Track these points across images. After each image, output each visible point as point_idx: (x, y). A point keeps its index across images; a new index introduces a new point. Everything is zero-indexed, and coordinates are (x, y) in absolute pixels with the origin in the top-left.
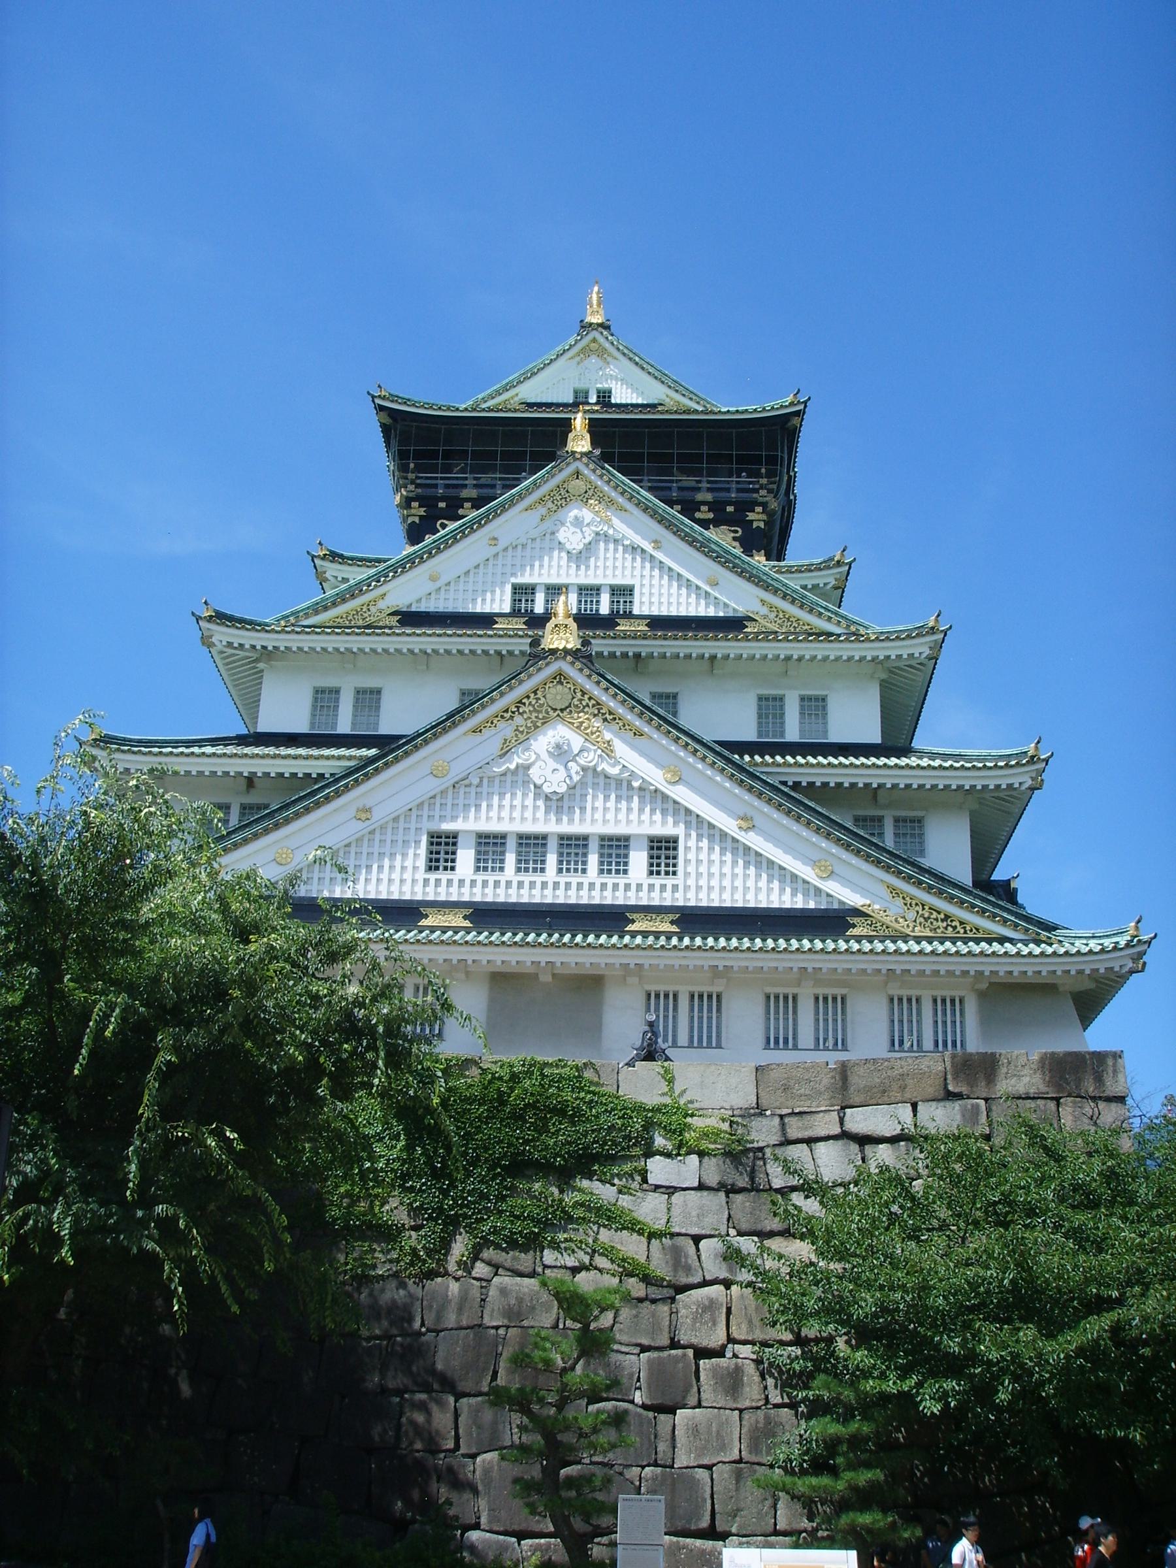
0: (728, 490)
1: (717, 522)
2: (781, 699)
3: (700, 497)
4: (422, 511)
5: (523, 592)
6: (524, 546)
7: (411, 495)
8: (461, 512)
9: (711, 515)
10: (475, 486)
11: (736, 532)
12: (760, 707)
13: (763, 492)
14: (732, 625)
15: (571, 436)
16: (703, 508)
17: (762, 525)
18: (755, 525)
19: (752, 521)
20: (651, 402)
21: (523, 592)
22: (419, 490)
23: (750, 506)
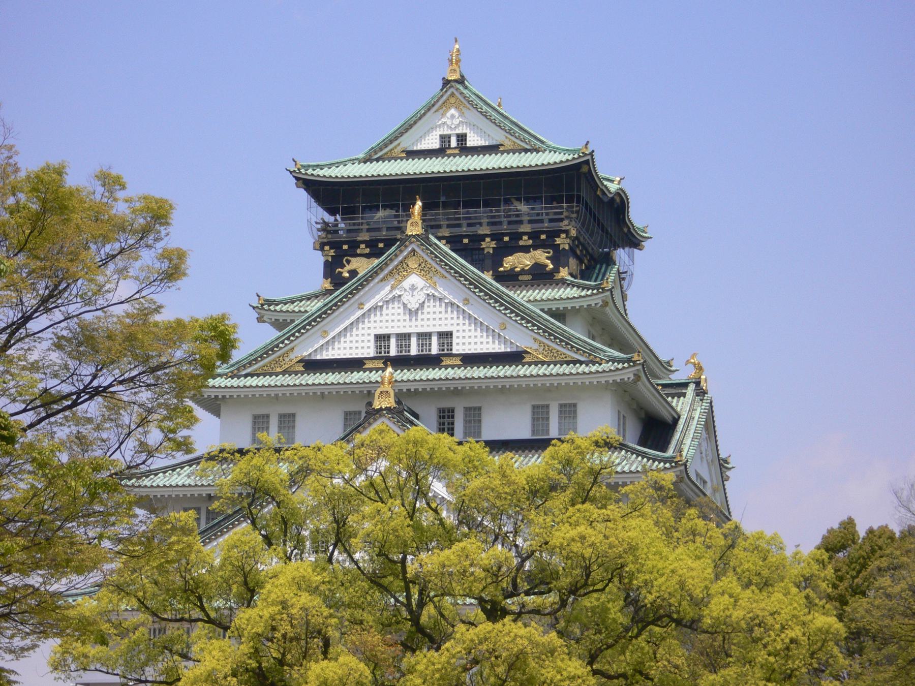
0: (542, 221)
1: (535, 247)
2: (548, 406)
3: (521, 230)
4: (332, 252)
5: (382, 339)
6: (381, 307)
7: (325, 240)
8: (359, 251)
9: (530, 242)
10: (368, 230)
11: (549, 253)
12: (534, 413)
13: (566, 222)
14: (515, 357)
15: (409, 223)
16: (525, 238)
17: (567, 247)
18: (561, 247)
19: (559, 245)
20: (494, 143)
21: (382, 339)
22: (330, 236)
23: (557, 233)
